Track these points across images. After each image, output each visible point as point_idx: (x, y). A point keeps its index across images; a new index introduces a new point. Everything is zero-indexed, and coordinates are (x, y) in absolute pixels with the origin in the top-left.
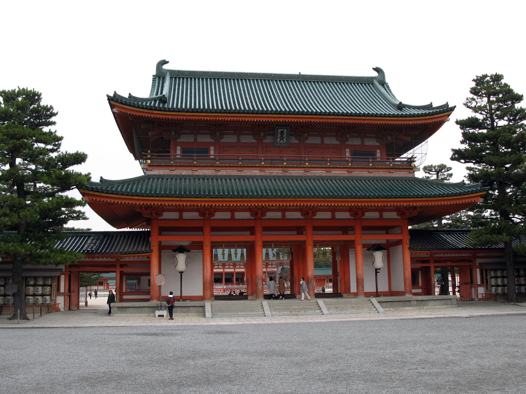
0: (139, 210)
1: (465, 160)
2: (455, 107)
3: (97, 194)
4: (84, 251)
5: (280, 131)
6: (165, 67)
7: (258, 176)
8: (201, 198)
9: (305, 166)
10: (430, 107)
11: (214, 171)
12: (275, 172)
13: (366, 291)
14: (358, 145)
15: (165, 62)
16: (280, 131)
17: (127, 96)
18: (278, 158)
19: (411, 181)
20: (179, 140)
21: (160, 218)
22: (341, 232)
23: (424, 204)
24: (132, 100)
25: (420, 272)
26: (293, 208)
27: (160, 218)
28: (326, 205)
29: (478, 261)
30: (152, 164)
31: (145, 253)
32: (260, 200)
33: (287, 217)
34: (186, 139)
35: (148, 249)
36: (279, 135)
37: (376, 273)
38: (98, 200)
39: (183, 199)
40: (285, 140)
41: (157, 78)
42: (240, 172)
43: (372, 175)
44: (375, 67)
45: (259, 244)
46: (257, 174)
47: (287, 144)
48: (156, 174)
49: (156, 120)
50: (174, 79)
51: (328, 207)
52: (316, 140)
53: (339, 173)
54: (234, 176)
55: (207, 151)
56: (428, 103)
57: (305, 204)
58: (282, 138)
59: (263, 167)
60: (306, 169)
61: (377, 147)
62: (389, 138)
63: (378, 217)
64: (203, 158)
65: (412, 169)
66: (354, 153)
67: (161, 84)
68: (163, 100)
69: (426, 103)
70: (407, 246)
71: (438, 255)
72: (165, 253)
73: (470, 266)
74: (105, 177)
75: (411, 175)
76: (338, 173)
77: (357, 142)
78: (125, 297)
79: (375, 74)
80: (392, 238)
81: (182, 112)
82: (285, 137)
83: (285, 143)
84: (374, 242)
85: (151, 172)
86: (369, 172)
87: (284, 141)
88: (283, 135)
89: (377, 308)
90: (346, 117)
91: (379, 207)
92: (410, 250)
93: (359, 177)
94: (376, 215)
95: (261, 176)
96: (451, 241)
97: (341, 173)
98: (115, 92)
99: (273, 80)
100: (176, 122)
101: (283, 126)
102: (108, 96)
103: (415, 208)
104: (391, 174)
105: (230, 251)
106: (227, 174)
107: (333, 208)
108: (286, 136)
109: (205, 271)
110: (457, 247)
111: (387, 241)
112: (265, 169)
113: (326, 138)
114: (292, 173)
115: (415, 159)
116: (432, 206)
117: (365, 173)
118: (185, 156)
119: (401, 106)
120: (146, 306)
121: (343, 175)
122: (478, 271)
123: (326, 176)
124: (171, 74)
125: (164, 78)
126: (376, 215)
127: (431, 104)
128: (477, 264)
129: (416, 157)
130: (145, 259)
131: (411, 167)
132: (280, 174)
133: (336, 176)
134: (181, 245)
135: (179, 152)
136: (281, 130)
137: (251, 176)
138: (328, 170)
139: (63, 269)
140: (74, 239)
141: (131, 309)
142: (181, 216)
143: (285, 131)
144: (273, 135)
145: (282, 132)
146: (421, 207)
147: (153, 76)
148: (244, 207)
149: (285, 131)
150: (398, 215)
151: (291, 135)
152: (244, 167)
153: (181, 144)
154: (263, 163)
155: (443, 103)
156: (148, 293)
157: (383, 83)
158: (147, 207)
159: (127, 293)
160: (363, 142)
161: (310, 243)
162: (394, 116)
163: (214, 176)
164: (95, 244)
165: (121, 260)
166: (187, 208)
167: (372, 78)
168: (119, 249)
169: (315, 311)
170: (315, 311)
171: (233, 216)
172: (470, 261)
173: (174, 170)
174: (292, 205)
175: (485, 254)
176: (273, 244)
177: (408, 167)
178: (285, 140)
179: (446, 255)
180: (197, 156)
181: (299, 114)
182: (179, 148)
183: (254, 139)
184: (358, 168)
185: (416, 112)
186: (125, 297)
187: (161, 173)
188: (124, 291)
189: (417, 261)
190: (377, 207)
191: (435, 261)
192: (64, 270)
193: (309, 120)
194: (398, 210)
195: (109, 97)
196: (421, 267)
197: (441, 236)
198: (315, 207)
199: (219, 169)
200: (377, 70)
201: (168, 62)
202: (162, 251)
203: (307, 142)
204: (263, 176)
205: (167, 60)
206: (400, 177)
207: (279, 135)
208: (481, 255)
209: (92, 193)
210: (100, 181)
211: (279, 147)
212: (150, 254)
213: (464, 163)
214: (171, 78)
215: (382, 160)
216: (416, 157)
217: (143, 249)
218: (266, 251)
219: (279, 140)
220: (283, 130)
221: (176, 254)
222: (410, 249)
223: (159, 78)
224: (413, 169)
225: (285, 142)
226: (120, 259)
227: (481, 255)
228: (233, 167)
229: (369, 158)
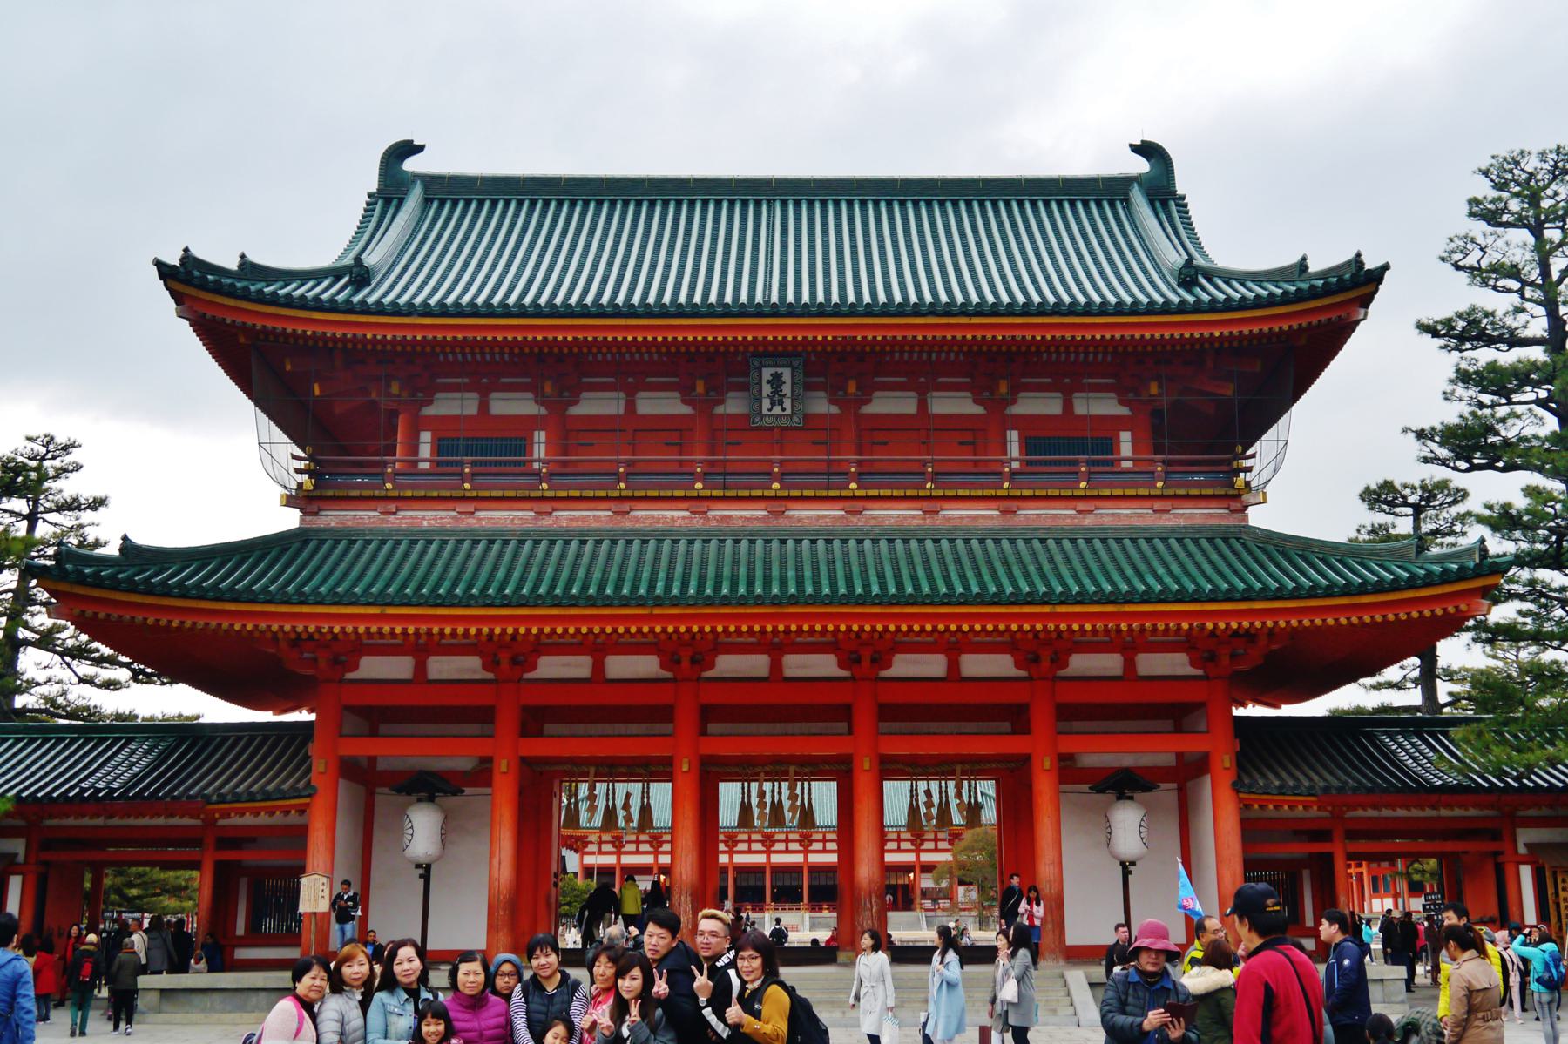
0: (272, 651)
1: (1468, 459)
3: (97, 593)
4: (84, 790)
5: (767, 373)
6: (412, 165)
7: (678, 531)
8: (453, 605)
9: (845, 493)
11: (532, 514)
12: (741, 517)
13: (1071, 940)
15: (408, 149)
16: (767, 373)
17: (232, 264)
18: (675, 468)
19: (1233, 541)
20: (428, 411)
21: (350, 676)
22: (1006, 726)
23: (1306, 622)
24: (249, 276)
25: (1306, 874)
26: (453, 641)
27: (350, 676)
28: (929, 628)
29: (1525, 836)
30: (317, 493)
31: (290, 798)
32: (657, 611)
33: (788, 673)
34: (453, 405)
35: (301, 785)
36: (767, 389)
37: (1126, 873)
38: (101, 615)
39: (390, 611)
40: (787, 403)
41: (380, 203)
42: (619, 518)
43: (1088, 521)
44: (1139, 143)
45: (685, 768)
46: (677, 524)
47: (797, 420)
48: (333, 524)
49: (340, 345)
50: (435, 204)
51: (936, 635)
52: (900, 404)
53: (969, 517)
54: (596, 530)
55: (522, 446)
56: (1294, 259)
57: (510, 630)
58: (776, 398)
59: (699, 498)
60: (849, 505)
61: (1118, 423)
62: (1154, 389)
63: (1119, 672)
64: (494, 469)
65: (1237, 497)
67: (387, 221)
68: (359, 275)
69: (1289, 259)
70: (1226, 781)
71: (1360, 813)
72: (384, 798)
73: (1496, 854)
74: (141, 539)
75: (1232, 521)
76: (961, 518)
77: (1040, 405)
78: (243, 953)
80: (1192, 745)
81: (409, 314)
82: (789, 395)
83: (791, 416)
84: (1127, 761)
85: (315, 518)
86: (1080, 512)
87: (784, 410)
88: (779, 386)
89: (1078, 1008)
90: (976, 320)
91: (1124, 634)
92: (1238, 792)
93: (1035, 530)
94: (1110, 663)
95: (690, 530)
96: (1411, 757)
97: (975, 518)
98: (186, 250)
99: (774, 200)
100: (369, 347)
101: (781, 355)
102: (159, 264)
103: (1250, 636)
104: (1158, 515)
105: (645, 794)
106: (574, 524)
107: (953, 639)
108: (793, 391)
109: (496, 861)
110: (1427, 781)
111: (1180, 756)
112: (703, 506)
113: (935, 394)
114: (799, 520)
115: (1249, 463)
116: (1315, 629)
117: (1063, 515)
118: (448, 463)
119: (1189, 276)
120: (260, 985)
121: (981, 524)
122: (1526, 872)
123: (919, 529)
124: (426, 189)
125: (401, 202)
126: (1110, 663)
127: (1302, 265)
128: (1522, 850)
129: (1253, 456)
130: (294, 818)
131: (1231, 492)
132: (757, 525)
133: (956, 529)
134: (421, 771)
135: (425, 451)
136: (773, 370)
137: (656, 530)
138: (926, 505)
139: (16, 855)
140: (105, 745)
141: (206, 1000)
142: (420, 668)
143: (786, 374)
144: (744, 387)
145: (776, 380)
146: (1272, 633)
147: (370, 195)
148: (639, 636)
149: (786, 374)
150: (1193, 664)
151: (809, 387)
152: (633, 499)
153: (436, 424)
154: (699, 485)
155: (1344, 256)
158: (297, 641)
159: (255, 937)
160: (1068, 405)
161: (867, 766)
162: (1167, 308)
163: (527, 532)
164: (134, 764)
165: (222, 822)
166: (443, 641)
168: (237, 785)
169: (844, 1013)
170: (844, 1013)
171: (598, 667)
172: (1495, 836)
173: (394, 514)
174: (818, 628)
175: (1545, 812)
176: (592, 770)
178: (787, 403)
179: (1444, 812)
180: (474, 464)
181: (810, 315)
182: (426, 437)
183: (537, 402)
184: (1034, 498)
185: (1237, 292)
186: (243, 953)
187: (350, 523)
188: (240, 930)
189: (1297, 833)
190: (1113, 635)
191: (1352, 835)
192: (21, 859)
193: (849, 334)
194: (1187, 643)
195: (165, 270)
196: (1311, 855)
197: (1382, 742)
198: (864, 636)
199: (547, 507)
201: (420, 149)
202: (379, 790)
203: (868, 409)
204: (698, 531)
205: (416, 142)
206: (1192, 527)
207: (767, 389)
208: (1531, 812)
209: (97, 593)
210: (120, 550)
211: (771, 429)
212: (307, 800)
213: (1467, 470)
214: (427, 201)
215: (1136, 470)
216: (1253, 456)
217: (286, 786)
218: (608, 800)
219: (766, 404)
220: (779, 370)
221: (410, 804)
222: (1237, 787)
223: (388, 202)
224: (1239, 496)
225: (788, 411)
226: (216, 820)
227: (1531, 812)
228: (595, 499)
229: (1076, 463)
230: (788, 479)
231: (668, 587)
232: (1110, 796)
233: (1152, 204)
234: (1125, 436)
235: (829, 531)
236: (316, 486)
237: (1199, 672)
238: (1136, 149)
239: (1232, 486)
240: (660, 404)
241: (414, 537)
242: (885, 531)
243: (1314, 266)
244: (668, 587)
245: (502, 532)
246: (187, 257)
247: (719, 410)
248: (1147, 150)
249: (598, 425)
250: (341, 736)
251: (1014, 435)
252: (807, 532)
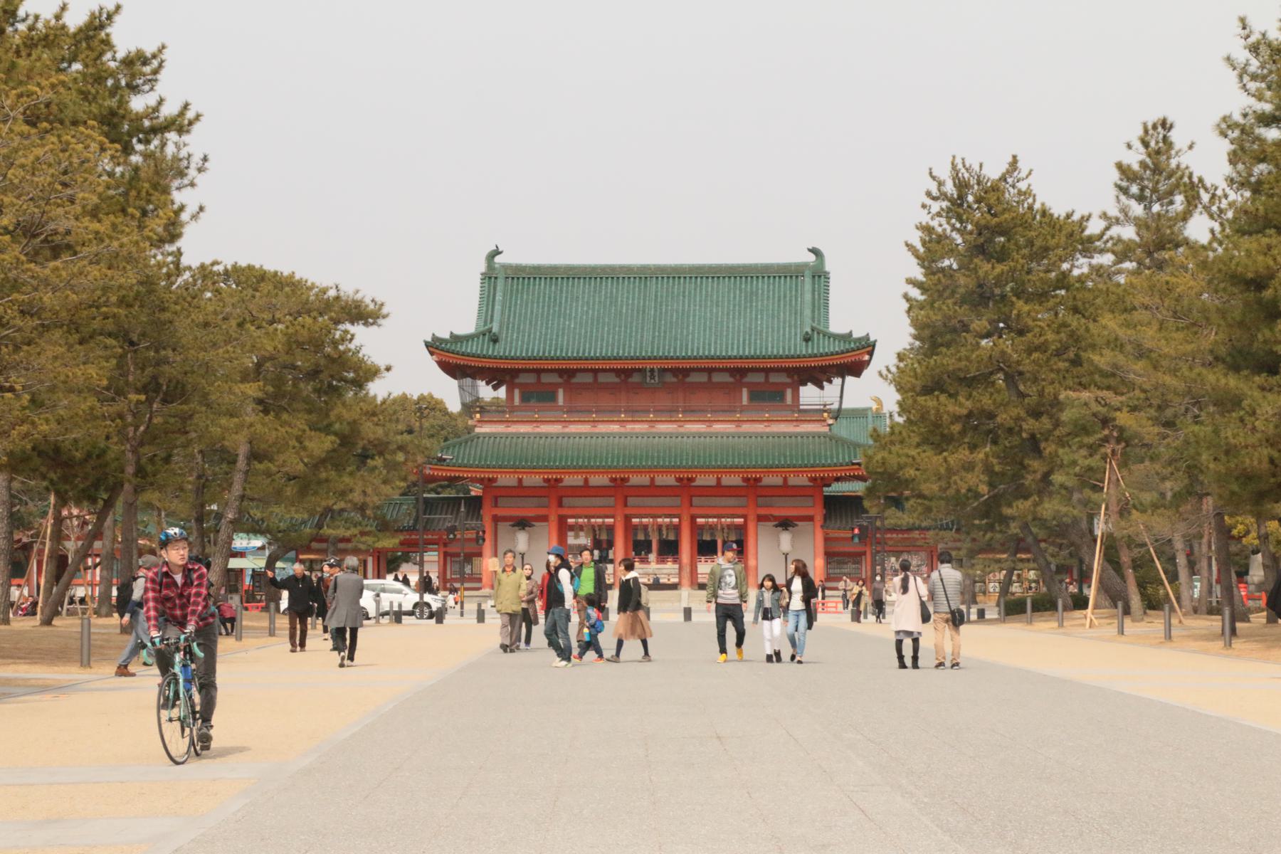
2: (875, 341)
10: (847, 337)
14: (759, 383)
20: (517, 381)
36: (648, 374)
40: (657, 378)
55: (553, 398)
56: (847, 331)
58: (652, 377)
60: (679, 424)
66: (752, 397)
68: (495, 340)
72: (504, 527)
79: (811, 258)
117: (759, 428)
127: (850, 334)
156: (480, 580)
157: (819, 275)
167: (806, 265)
178: (657, 378)
188: (448, 577)
200: (815, 251)
207: (648, 374)
219: (648, 379)
231: (612, 461)
232: (780, 529)
233: (814, 277)
235: (672, 433)
241: (518, 435)
242: (691, 433)
243: (855, 335)
244: (612, 461)
245: (551, 434)
246: (435, 338)
247: (630, 380)
248: (815, 251)
252: (663, 434)
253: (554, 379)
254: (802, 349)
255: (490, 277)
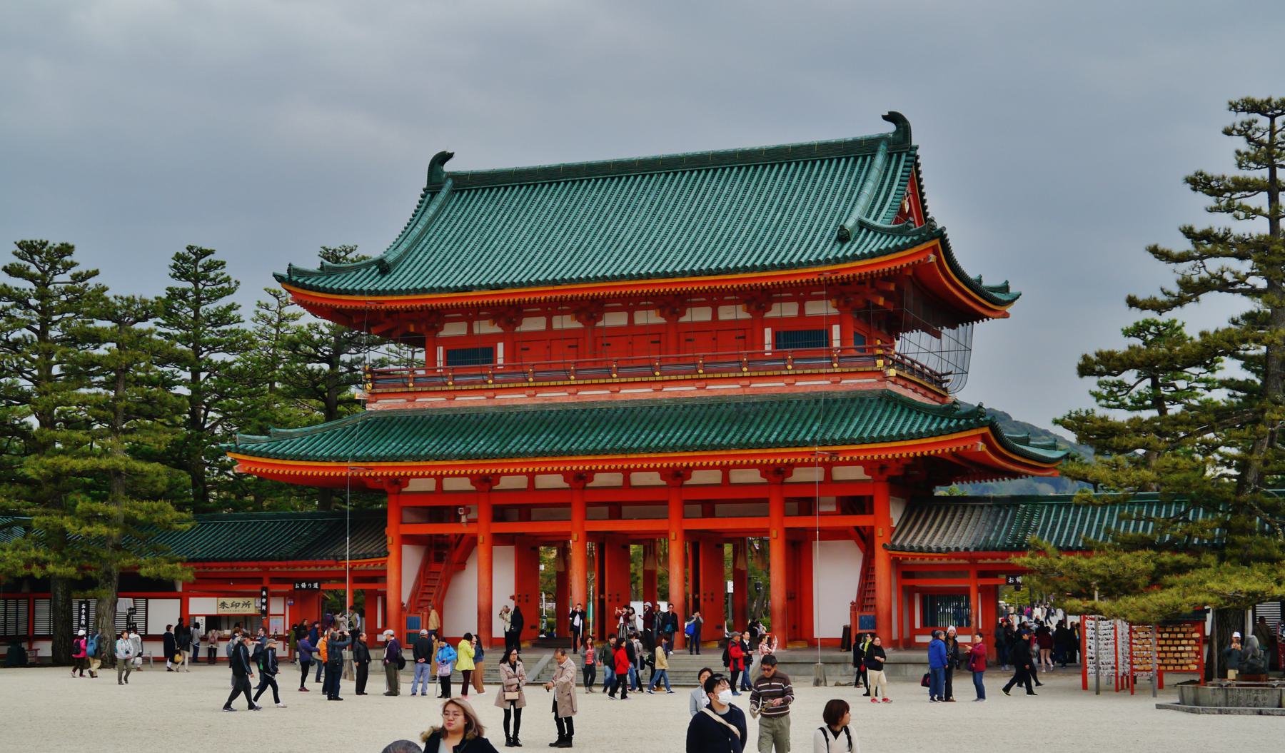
20: (442, 334)
30: (374, 391)
34: (454, 330)
55: (490, 354)
77: (788, 310)
132: (603, 399)
177: (870, 369)
182: (440, 350)
214: (453, 192)
230: (621, 371)
234: (836, 329)
236: (373, 387)
237: (869, 477)
238: (885, 118)
239: (876, 365)
240: (565, 323)
247: (600, 324)
249: (533, 336)
250: (402, 523)
251: (768, 333)
253: (485, 328)
254: (835, 252)
255: (432, 188)
